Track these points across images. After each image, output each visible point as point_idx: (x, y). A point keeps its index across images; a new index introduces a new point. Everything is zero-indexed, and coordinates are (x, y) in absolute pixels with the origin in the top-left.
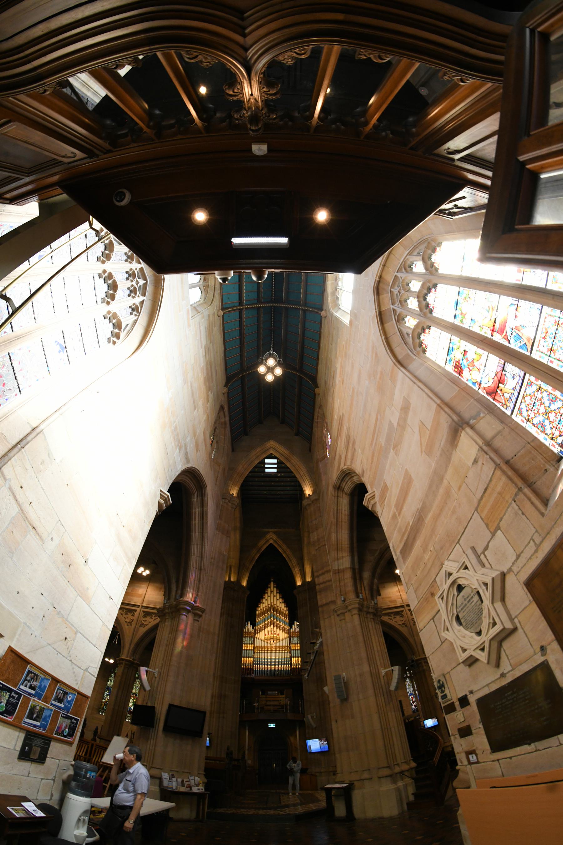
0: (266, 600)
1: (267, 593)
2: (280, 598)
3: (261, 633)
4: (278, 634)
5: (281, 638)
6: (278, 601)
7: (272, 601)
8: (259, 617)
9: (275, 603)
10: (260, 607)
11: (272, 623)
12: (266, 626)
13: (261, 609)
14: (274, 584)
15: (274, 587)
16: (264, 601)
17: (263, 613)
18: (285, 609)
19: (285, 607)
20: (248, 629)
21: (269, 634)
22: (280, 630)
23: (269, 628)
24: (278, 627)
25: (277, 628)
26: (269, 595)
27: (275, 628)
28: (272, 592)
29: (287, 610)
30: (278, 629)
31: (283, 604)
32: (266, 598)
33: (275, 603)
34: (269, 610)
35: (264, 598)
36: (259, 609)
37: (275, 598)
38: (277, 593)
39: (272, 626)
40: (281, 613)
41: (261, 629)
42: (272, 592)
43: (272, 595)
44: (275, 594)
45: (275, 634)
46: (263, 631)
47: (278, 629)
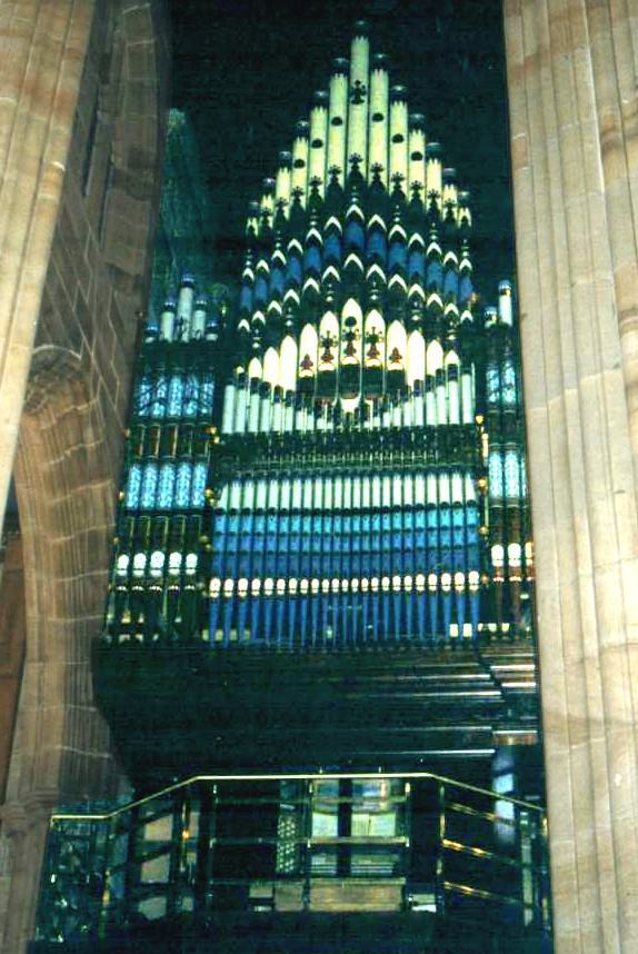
0: (318, 144)
1: (326, 104)
2: (412, 126)
3: (271, 352)
4: (396, 356)
5: (414, 375)
6: (399, 150)
7: (357, 148)
8: (263, 246)
9: (378, 156)
10: (272, 190)
11: (355, 285)
12: (311, 310)
13: (280, 204)
14: (372, 52)
15: (373, 66)
16: (301, 149)
17: (296, 223)
18: (451, 194)
19: (447, 180)
20: (178, 323)
21: (327, 358)
22: (410, 327)
23: (329, 322)
24: (394, 306)
25: (388, 321)
26: (338, 109)
27: (375, 319)
28: (357, 95)
29: (463, 203)
30: (397, 327)
31: (435, 168)
32: (318, 132)
33: (378, 156)
34: (336, 199)
35: (306, 133)
36: (268, 203)
37: (379, 129)
38: (393, 98)
39: (352, 308)
40: (419, 216)
41: (273, 334)
42: (357, 95)
43: (359, 112)
44: (379, 102)
45: (373, 354)
46: (288, 342)
47: (397, 327)
